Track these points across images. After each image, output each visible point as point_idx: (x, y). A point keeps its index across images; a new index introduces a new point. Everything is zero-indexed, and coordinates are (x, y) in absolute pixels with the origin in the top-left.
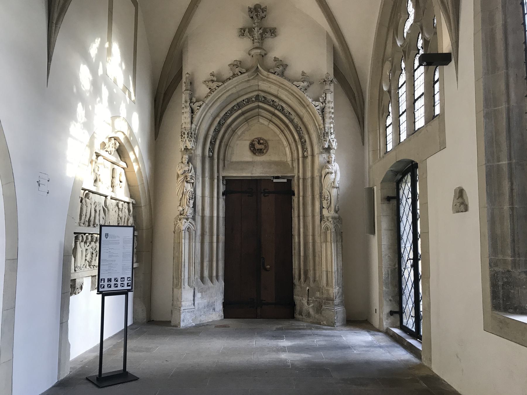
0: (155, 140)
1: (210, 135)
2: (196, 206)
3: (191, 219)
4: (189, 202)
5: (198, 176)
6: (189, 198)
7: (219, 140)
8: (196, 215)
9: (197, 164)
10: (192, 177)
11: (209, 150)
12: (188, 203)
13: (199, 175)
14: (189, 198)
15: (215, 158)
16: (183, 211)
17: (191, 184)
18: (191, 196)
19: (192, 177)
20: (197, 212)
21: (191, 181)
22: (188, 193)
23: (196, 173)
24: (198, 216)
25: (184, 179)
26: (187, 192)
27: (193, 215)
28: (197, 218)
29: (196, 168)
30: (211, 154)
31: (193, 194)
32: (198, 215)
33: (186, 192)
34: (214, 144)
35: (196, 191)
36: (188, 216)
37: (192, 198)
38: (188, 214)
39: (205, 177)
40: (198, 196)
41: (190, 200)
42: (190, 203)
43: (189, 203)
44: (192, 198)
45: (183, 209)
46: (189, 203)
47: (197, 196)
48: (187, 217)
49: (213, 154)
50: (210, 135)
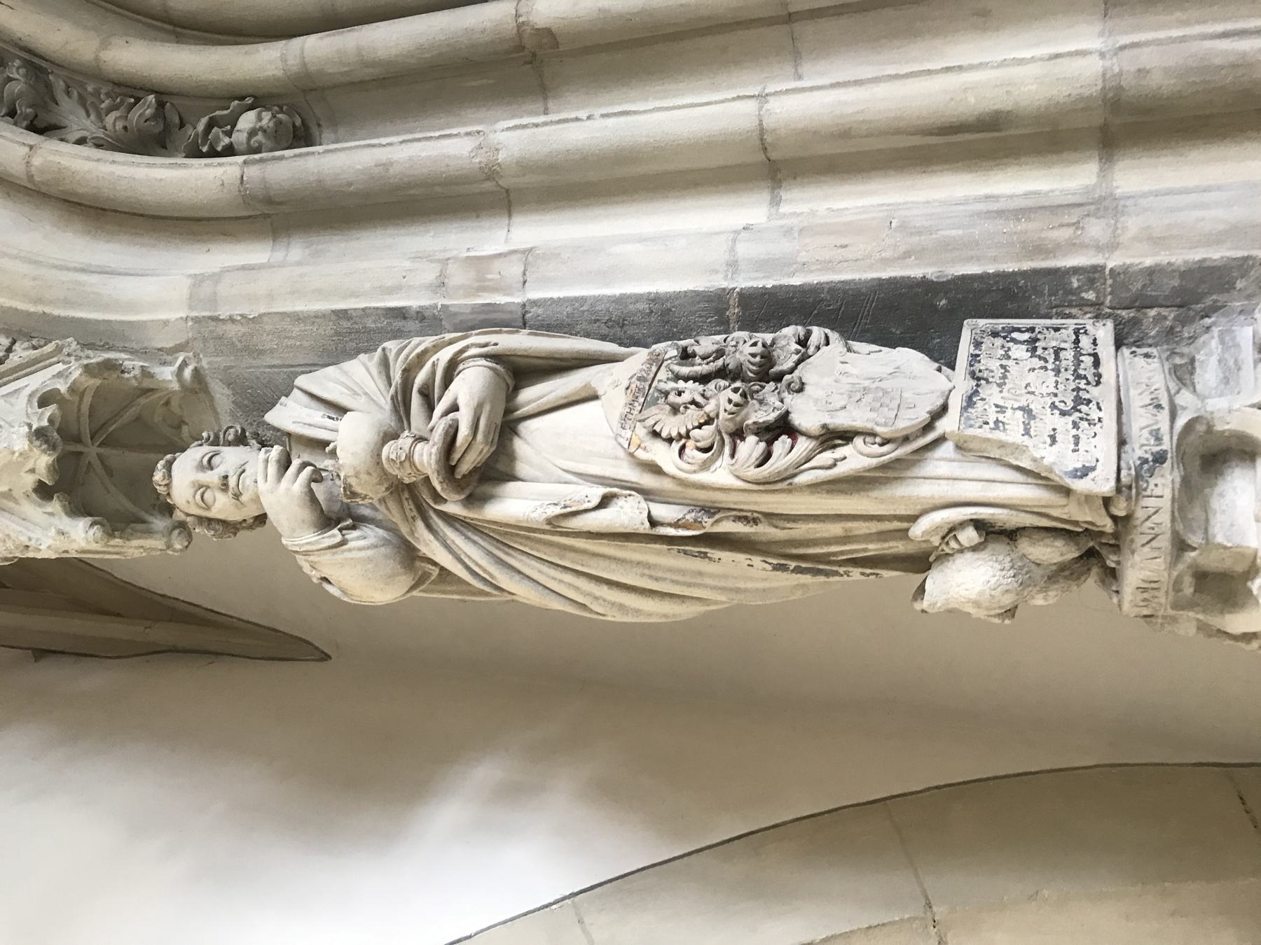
0: (326, 657)
1: (37, 161)
2: (916, 272)
3: (1184, 374)
4: (833, 437)
5: (440, 285)
6: (751, 447)
7: (105, 45)
8: (1092, 275)
9: (300, 307)
10: (416, 401)
11: (213, 154)
12: (854, 458)
13: (429, 274)
14: (751, 447)
15: (293, 63)
16: (1011, 535)
17: (532, 395)
18: (722, 397)
19: (416, 401)
20: (1040, 249)
21: (464, 419)
22: (665, 456)
23: (401, 313)
24: (1132, 224)
25: (449, 519)
26: (648, 481)
27: (1104, 332)
28: (1157, 241)
29: (343, 314)
30: (247, 121)
31: (686, 356)
32: (1096, 229)
33: (647, 494)
34: (158, 93)
35: (655, 299)
36: (1140, 448)
37: (766, 371)
38: (1100, 447)
39: (490, 173)
40: (733, 266)
41: (783, 427)
42: (842, 421)
43: (846, 436)
44: (766, 371)
45: (969, 536)
46: (846, 436)
47: (746, 281)
48: (1164, 484)
49: (257, 97)
50: (37, 161)
